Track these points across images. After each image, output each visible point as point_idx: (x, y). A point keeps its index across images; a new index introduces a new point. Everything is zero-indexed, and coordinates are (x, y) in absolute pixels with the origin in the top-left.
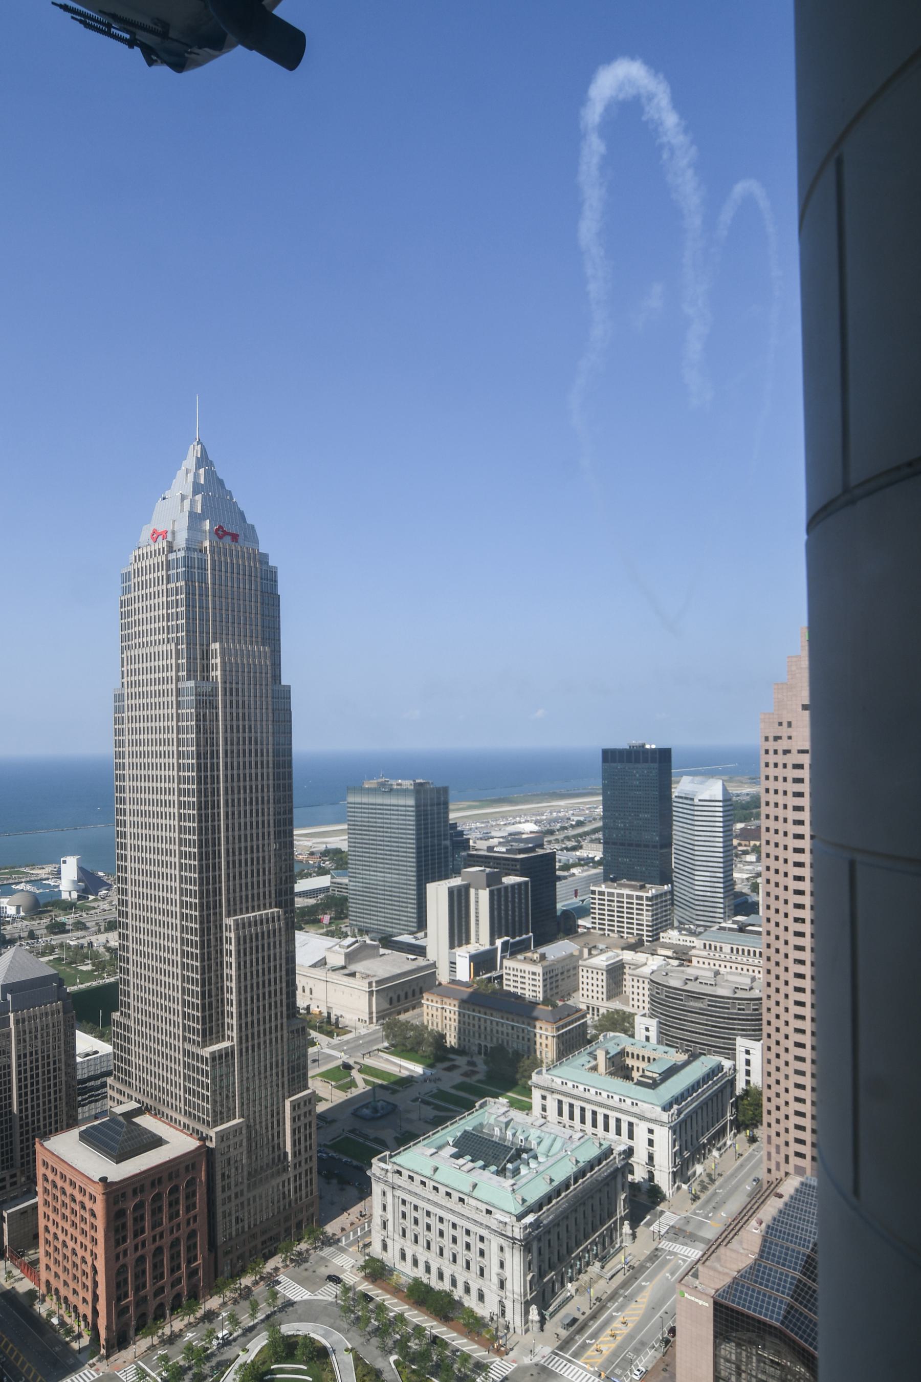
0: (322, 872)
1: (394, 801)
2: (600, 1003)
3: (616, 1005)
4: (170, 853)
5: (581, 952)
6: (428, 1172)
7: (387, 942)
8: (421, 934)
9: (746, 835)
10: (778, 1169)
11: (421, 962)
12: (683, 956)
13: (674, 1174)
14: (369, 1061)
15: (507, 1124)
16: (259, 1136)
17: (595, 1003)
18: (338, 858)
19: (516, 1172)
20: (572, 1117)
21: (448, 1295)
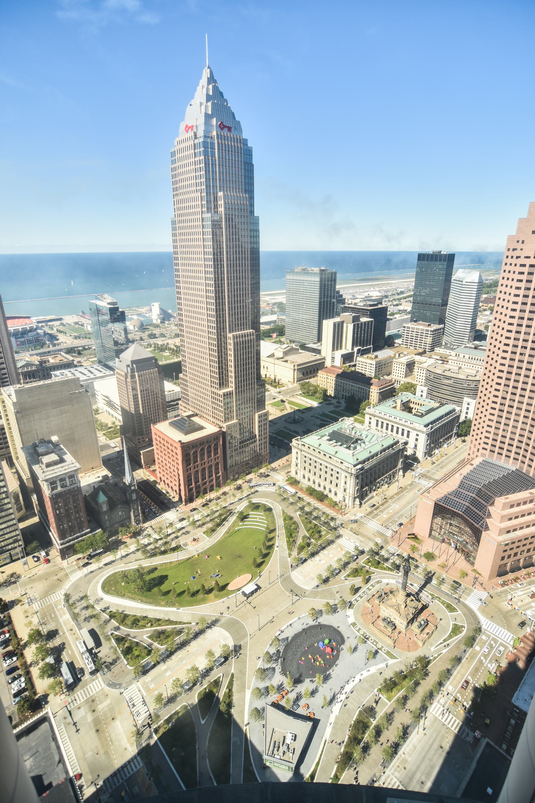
0: (273, 313)
1: (309, 279)
2: (401, 379)
3: (409, 380)
4: (202, 302)
5: (395, 355)
6: (317, 446)
7: (303, 347)
8: (319, 344)
9: (487, 301)
10: (473, 454)
11: (318, 357)
12: (444, 360)
13: (425, 453)
14: (292, 399)
15: (353, 428)
16: (244, 427)
17: (399, 379)
18: (281, 306)
19: (355, 448)
20: (382, 427)
21: (322, 494)
